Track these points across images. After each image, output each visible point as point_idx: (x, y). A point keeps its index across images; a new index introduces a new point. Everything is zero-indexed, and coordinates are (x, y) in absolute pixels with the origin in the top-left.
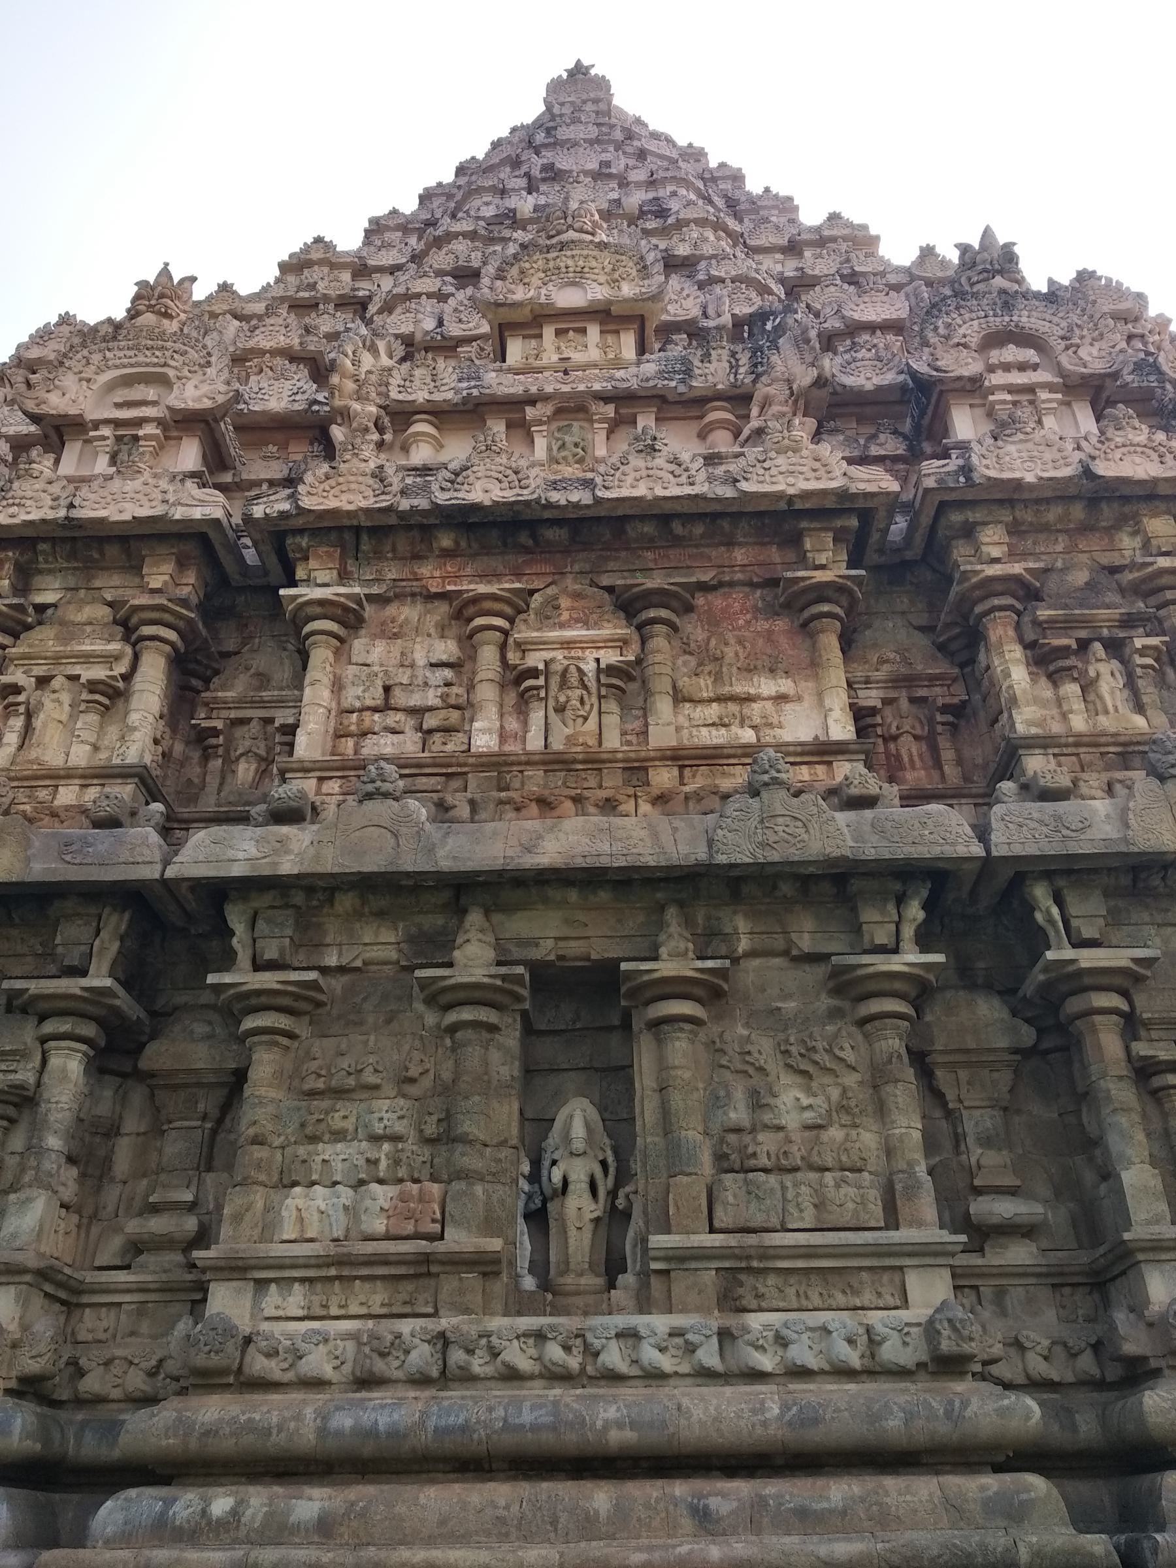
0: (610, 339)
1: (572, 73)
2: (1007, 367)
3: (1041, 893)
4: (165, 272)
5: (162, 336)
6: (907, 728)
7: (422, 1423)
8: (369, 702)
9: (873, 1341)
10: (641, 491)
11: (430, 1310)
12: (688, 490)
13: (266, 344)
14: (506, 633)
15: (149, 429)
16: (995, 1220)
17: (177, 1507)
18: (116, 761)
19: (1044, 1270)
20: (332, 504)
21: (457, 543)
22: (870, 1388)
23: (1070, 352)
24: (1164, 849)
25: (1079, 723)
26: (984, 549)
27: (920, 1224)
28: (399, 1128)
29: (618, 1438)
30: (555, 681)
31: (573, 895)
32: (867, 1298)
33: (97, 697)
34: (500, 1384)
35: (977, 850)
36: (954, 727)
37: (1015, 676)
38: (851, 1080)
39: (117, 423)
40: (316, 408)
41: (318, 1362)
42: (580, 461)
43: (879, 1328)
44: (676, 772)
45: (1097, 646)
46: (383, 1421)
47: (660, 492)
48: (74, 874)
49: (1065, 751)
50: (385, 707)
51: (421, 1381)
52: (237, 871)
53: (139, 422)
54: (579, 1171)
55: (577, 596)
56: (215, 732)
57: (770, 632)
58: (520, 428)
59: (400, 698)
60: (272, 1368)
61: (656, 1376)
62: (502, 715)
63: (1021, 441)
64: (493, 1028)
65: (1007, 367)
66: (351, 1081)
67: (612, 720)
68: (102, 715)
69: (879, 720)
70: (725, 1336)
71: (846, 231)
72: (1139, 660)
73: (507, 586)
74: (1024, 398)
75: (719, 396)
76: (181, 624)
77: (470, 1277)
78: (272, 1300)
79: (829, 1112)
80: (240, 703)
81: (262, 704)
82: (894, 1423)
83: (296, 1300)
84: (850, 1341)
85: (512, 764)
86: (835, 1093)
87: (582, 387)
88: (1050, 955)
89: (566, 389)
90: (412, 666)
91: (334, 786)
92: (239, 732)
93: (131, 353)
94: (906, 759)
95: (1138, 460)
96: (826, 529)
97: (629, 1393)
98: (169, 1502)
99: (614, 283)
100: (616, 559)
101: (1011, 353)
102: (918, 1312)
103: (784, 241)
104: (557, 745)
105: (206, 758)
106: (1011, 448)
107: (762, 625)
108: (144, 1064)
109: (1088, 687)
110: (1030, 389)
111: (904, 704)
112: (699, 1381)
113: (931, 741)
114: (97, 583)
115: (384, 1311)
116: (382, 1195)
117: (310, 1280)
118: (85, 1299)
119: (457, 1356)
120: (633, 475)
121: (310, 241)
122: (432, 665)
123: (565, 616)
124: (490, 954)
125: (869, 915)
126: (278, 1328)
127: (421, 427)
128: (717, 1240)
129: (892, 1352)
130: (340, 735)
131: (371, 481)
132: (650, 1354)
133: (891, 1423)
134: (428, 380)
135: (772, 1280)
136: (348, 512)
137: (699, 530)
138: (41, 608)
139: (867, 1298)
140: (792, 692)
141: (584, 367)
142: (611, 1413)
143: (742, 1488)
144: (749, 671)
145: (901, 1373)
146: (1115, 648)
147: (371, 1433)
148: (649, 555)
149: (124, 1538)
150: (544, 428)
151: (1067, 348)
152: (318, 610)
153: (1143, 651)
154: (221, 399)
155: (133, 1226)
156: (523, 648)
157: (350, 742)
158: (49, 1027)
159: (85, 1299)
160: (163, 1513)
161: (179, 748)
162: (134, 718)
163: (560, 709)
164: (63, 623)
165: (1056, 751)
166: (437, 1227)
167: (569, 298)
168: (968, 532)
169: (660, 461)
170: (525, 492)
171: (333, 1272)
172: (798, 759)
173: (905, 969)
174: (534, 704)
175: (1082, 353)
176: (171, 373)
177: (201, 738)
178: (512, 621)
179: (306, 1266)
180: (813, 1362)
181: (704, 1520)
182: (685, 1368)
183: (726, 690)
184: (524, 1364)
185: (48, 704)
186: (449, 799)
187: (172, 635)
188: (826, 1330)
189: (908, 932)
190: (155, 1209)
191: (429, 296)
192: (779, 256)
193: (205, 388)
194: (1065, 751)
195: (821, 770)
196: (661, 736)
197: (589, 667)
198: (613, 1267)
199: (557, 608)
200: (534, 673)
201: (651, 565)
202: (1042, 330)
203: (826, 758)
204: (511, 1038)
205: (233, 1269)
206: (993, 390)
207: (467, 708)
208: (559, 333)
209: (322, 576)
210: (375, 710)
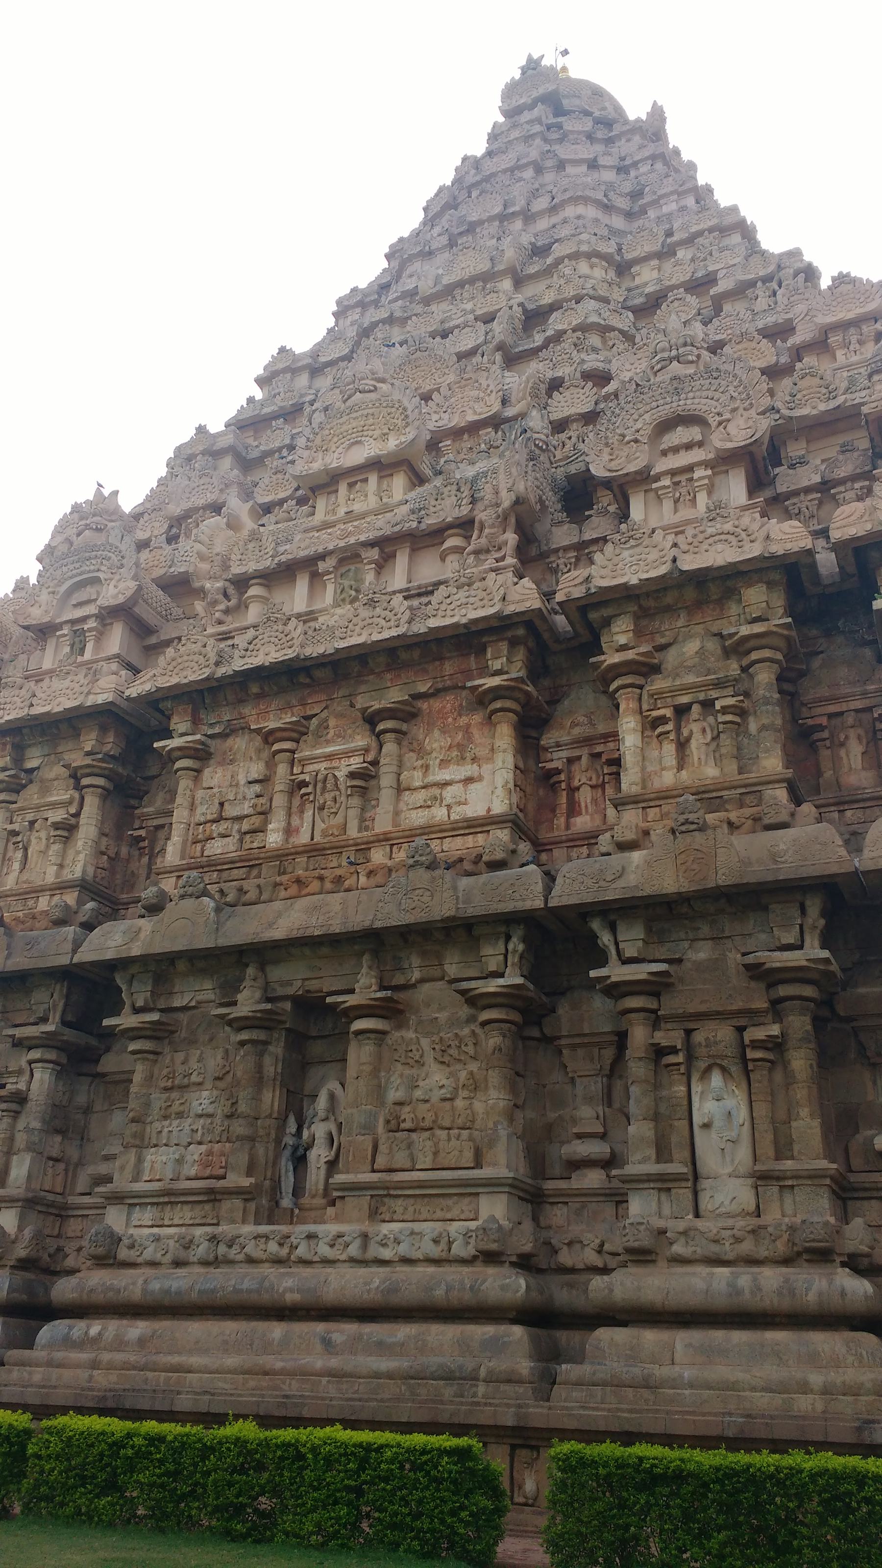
1: (524, 70)
2: (675, 450)
4: (99, 493)
6: (584, 780)
7: (191, 1288)
8: (209, 817)
11: (215, 1221)
12: (394, 633)
14: (293, 752)
15: (91, 624)
16: (578, 1157)
17: (74, 1330)
19: (607, 1191)
20: (174, 680)
21: (262, 688)
23: (721, 428)
24: (664, 892)
25: (668, 779)
26: (616, 638)
28: (210, 1110)
29: (291, 1298)
30: (319, 785)
31: (307, 951)
32: (455, 1213)
33: (59, 832)
34: (247, 1266)
35: (539, 903)
37: (627, 744)
38: (474, 1066)
39: (73, 622)
43: (453, 1234)
44: (388, 848)
47: (376, 637)
49: (652, 804)
51: (205, 1263)
52: (109, 955)
53: (84, 619)
55: (340, 716)
57: (468, 726)
58: (315, 577)
59: (230, 811)
61: (327, 1262)
62: (289, 815)
63: (632, 547)
65: (675, 450)
66: (186, 1081)
67: (353, 814)
68: (65, 843)
69: (563, 777)
70: (365, 1237)
73: (288, 720)
74: (683, 478)
75: (450, 526)
76: (106, 772)
79: (456, 1089)
82: (439, 1293)
83: (147, 1216)
84: (436, 1241)
85: (287, 855)
86: (463, 1075)
87: (352, 540)
89: (342, 544)
90: (237, 785)
93: (77, 565)
94: (583, 805)
95: (720, 547)
96: (502, 640)
98: (71, 1328)
99: (384, 437)
100: (366, 682)
101: (680, 435)
103: (656, 247)
105: (141, 855)
106: (626, 554)
107: (464, 720)
108: (100, 1069)
109: (682, 745)
110: (690, 469)
111: (584, 760)
112: (352, 1264)
114: (60, 749)
115: (191, 1222)
116: (196, 1152)
117: (157, 1204)
118: (71, 1213)
119: (222, 1249)
120: (361, 624)
121: (275, 352)
122: (250, 783)
123: (332, 732)
124: (258, 994)
128: (375, 1177)
129: (458, 1249)
132: (324, 1250)
133: (438, 1292)
134: (257, 552)
135: (400, 1202)
136: (185, 684)
137: (416, 653)
138: (31, 771)
139: (455, 1213)
140: (476, 775)
141: (363, 516)
142: (289, 1283)
143: (351, 1328)
145: (463, 1262)
147: (167, 1292)
148: (389, 676)
149: (51, 1346)
150: (332, 576)
151: (720, 424)
152: (179, 753)
154: (129, 593)
156: (303, 762)
157: (199, 847)
159: (71, 1213)
160: (68, 1333)
161: (124, 851)
162: (80, 843)
165: (643, 805)
166: (221, 1172)
168: (607, 622)
170: (290, 651)
171: (166, 1199)
172: (467, 831)
173: (498, 990)
176: (101, 575)
178: (297, 741)
179: (153, 1196)
181: (327, 1343)
182: (343, 1257)
183: (431, 779)
184: (257, 1254)
185: (34, 841)
186: (245, 888)
187: (101, 781)
188: (421, 1234)
192: (655, 262)
193: (122, 585)
194: (652, 804)
195: (480, 838)
199: (327, 727)
200: (305, 784)
201: (389, 685)
202: (705, 408)
203: (485, 829)
204: (277, 1049)
205: (117, 1198)
206: (657, 478)
207: (265, 814)
208: (351, 485)
209: (182, 727)
210: (214, 821)
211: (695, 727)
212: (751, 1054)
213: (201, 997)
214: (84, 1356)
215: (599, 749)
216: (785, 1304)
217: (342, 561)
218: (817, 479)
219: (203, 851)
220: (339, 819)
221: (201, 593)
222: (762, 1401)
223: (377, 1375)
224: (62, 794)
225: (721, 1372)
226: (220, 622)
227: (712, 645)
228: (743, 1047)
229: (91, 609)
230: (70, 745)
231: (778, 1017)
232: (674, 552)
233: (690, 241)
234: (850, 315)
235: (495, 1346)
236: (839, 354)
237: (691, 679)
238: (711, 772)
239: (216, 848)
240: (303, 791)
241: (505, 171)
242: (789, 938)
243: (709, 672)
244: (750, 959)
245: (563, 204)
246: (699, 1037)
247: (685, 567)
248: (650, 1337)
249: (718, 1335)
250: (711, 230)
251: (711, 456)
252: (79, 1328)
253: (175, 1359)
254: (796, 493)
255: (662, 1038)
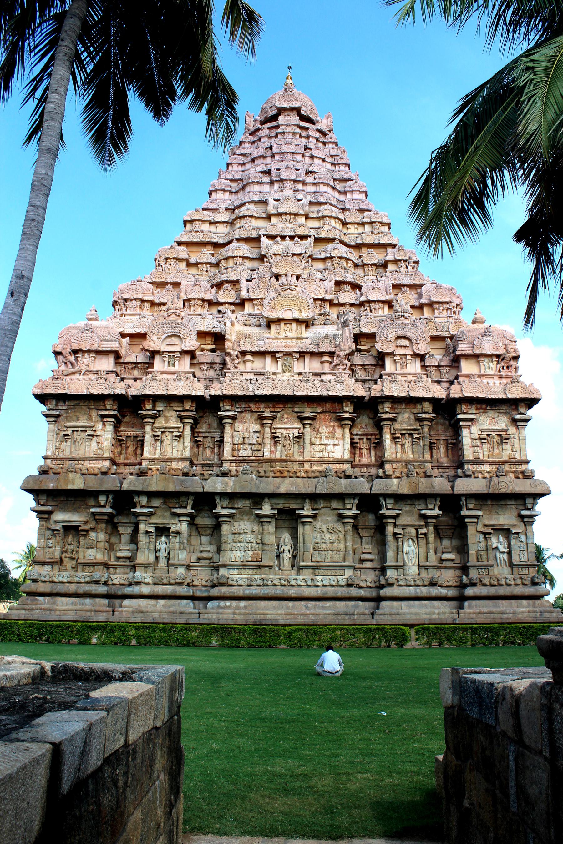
0: (299, 327)
2: (401, 347)
3: (381, 499)
5: (178, 323)
9: (338, 581)
10: (304, 393)
13: (196, 297)
18: (184, 456)
22: (336, 588)
25: (399, 455)
27: (349, 561)
28: (252, 541)
35: (369, 492)
36: (375, 448)
39: (169, 352)
40: (214, 329)
41: (240, 582)
42: (290, 371)
45: (407, 435)
46: (254, 592)
48: (186, 490)
50: (244, 443)
52: (218, 491)
53: (174, 352)
54: (287, 548)
55: (287, 414)
56: (200, 441)
59: (247, 441)
60: (234, 583)
61: (300, 586)
64: (270, 522)
71: (380, 220)
72: (415, 440)
74: (403, 357)
77: (267, 569)
78: (231, 571)
80: (206, 433)
81: (210, 433)
83: (236, 571)
88: (381, 512)
89: (287, 350)
91: (233, 465)
92: (206, 440)
97: (295, 588)
102: (346, 576)
104: (284, 457)
106: (393, 385)
107: (332, 424)
109: (402, 445)
110: (406, 355)
111: (365, 440)
113: (370, 450)
114: (172, 405)
119: (265, 582)
123: (286, 420)
125: (347, 502)
126: (233, 576)
127: (249, 357)
130: (233, 450)
131: (239, 386)
138: (159, 411)
141: (291, 339)
142: (292, 592)
144: (327, 438)
145: (342, 586)
146: (411, 435)
153: (416, 438)
155: (200, 555)
158: (182, 518)
163: (284, 446)
164: (165, 416)
167: (288, 315)
169: (310, 384)
174: (278, 444)
175: (419, 346)
176: (182, 336)
177: (196, 442)
178: (273, 420)
180: (327, 584)
183: (322, 442)
187: (191, 421)
189: (354, 505)
190: (202, 552)
191: (240, 257)
192: (356, 226)
193: (192, 343)
195: (341, 465)
196: (307, 457)
197: (291, 436)
198: (293, 566)
200: (278, 437)
209: (228, 408)
211: (407, 441)
212: (420, 536)
213: (245, 505)
214: (230, 611)
215: (369, 437)
216: (428, 595)
217: (284, 355)
218: (437, 364)
219: (238, 454)
220: (291, 451)
221: (228, 354)
222: (425, 616)
223: (326, 614)
224: (174, 423)
225: (413, 610)
226: (236, 367)
227: (412, 417)
228: (417, 534)
229: (177, 349)
230: (176, 404)
231: (426, 526)
232: (408, 389)
233: (371, 223)
234: (441, 301)
235: (356, 607)
236: (436, 311)
237: (405, 426)
238: (411, 456)
239: (243, 454)
240: (277, 439)
241: (290, 153)
242: (431, 507)
243: (411, 425)
244: (423, 512)
245: (319, 183)
246: (406, 531)
247: (412, 395)
248: (395, 603)
249: (412, 602)
250: (379, 222)
251: (412, 353)
252: (222, 603)
253: (262, 612)
254: (430, 366)
255: (396, 530)
